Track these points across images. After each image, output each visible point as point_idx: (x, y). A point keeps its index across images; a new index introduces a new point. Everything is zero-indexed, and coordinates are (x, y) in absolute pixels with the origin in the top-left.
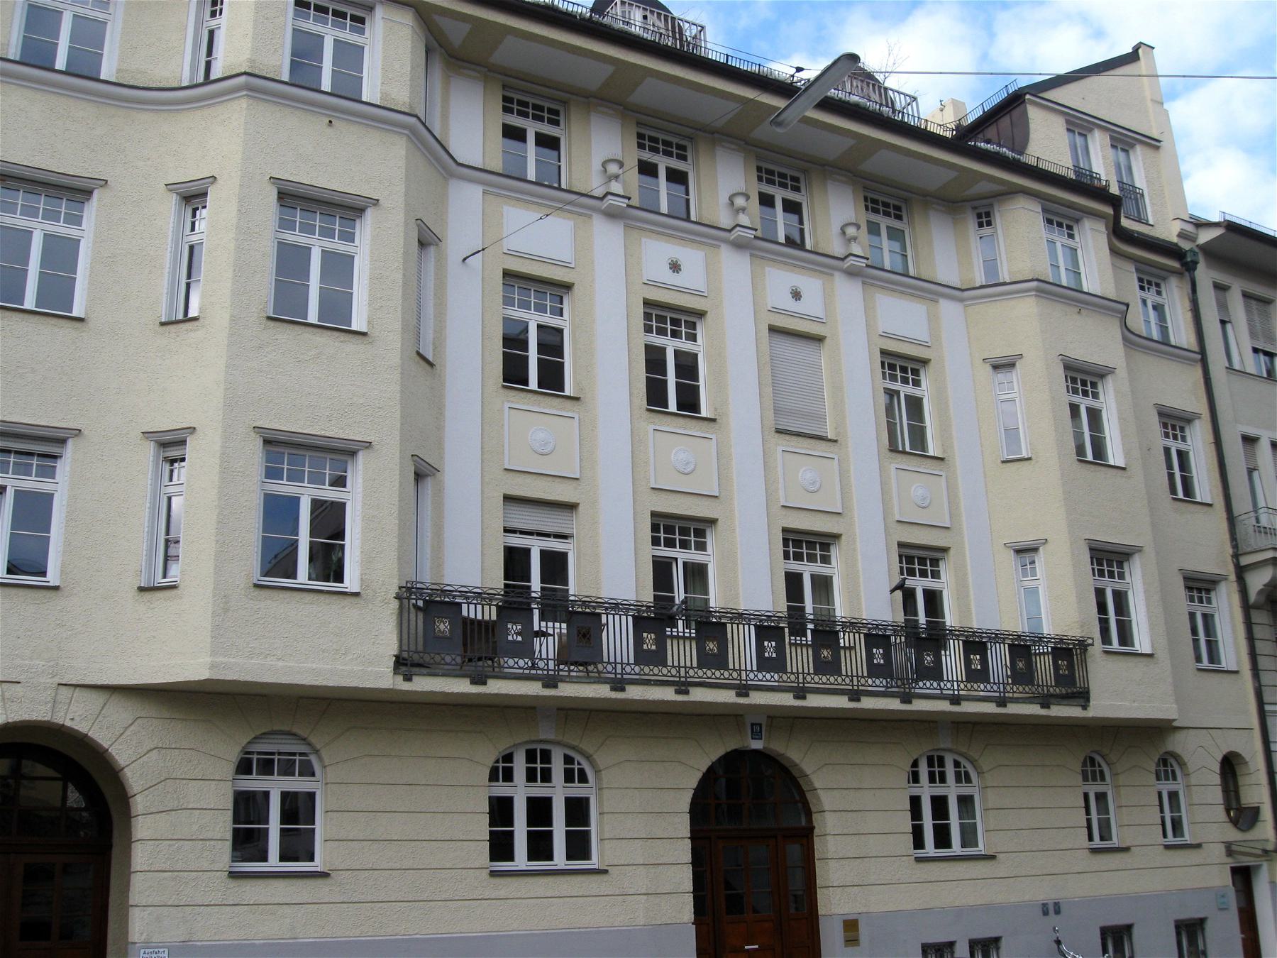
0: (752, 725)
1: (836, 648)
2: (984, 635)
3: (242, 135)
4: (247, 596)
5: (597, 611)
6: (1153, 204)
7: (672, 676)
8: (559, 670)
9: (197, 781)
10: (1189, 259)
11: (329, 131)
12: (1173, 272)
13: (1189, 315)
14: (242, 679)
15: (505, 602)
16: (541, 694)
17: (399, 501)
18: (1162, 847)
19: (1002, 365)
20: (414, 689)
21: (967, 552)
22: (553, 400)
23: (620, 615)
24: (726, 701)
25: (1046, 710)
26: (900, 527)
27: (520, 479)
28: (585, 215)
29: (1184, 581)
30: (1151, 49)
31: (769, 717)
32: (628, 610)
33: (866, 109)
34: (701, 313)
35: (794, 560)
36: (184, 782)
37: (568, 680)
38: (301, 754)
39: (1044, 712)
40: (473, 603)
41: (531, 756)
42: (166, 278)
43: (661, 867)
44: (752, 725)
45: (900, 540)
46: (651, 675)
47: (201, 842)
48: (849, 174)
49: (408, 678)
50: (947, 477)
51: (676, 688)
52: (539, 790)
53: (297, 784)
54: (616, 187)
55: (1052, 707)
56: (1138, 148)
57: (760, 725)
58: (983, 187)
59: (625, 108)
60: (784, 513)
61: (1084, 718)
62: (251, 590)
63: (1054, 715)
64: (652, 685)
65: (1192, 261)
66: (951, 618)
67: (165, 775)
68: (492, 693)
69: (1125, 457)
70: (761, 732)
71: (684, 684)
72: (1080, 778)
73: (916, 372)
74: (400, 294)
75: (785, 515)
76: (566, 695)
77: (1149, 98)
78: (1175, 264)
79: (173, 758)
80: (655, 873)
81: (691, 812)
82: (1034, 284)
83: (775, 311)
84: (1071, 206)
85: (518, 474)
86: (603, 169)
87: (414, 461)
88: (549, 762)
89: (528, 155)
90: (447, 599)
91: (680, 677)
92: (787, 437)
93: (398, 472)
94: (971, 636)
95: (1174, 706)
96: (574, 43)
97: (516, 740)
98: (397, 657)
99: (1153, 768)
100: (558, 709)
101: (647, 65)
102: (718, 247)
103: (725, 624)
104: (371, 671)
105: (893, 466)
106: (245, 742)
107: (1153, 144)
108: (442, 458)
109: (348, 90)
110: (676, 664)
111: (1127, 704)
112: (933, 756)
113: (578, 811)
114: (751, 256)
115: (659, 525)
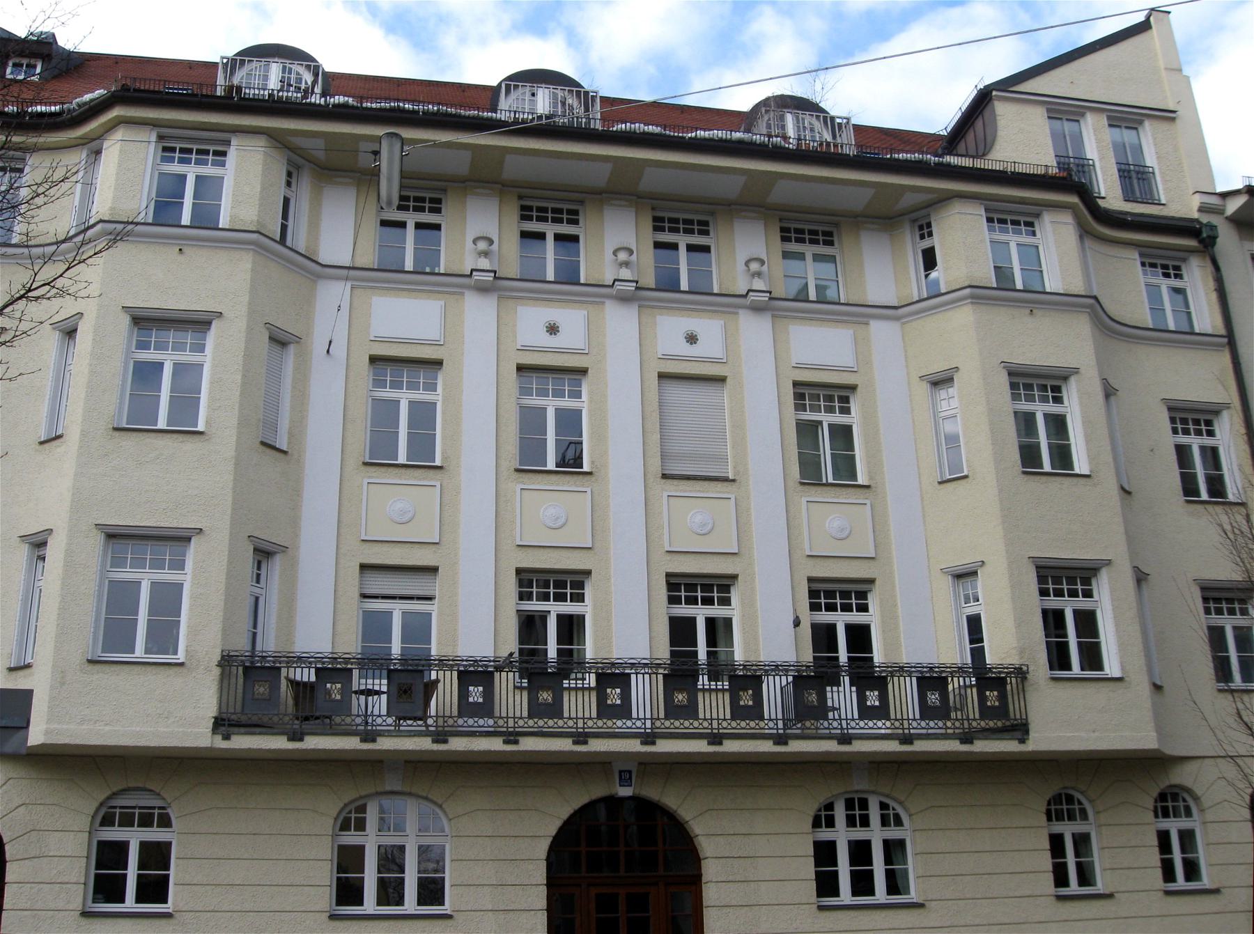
0: (620, 772)
1: (693, 692)
2: (913, 669)
3: (101, 274)
4: (81, 671)
5: (626, 671)
6: (1165, 181)
7: (638, 728)
8: (400, 725)
9: (58, 832)
10: (1204, 235)
11: (181, 258)
12: (1191, 251)
13: (1214, 296)
14: (72, 742)
15: (558, 669)
16: (359, 748)
17: (226, 579)
18: (1162, 892)
19: (941, 381)
20: (232, 747)
21: (897, 582)
22: (415, 472)
23: (780, 676)
24: (561, 749)
25: (969, 745)
26: (812, 561)
27: (377, 548)
28: (597, 303)
29: (1202, 591)
30: (1166, 14)
31: (640, 764)
32: (787, 671)
33: (752, 143)
34: (584, 370)
35: (685, 604)
36: (47, 833)
37: (386, 734)
38: (160, 808)
39: (436, 747)
40: (235, 666)
41: (849, 804)
42: (46, 406)
43: (512, 913)
44: (620, 772)
45: (810, 575)
46: (555, 728)
47: (59, 885)
48: (761, 209)
49: (227, 737)
50: (736, 499)
51: (504, 738)
52: (859, 834)
53: (155, 834)
54: (759, 284)
55: (975, 741)
56: (1147, 124)
57: (630, 772)
58: (908, 200)
59: (503, 186)
60: (668, 558)
61: (1021, 753)
62: (86, 665)
63: (978, 750)
64: (478, 736)
65: (1209, 237)
66: (590, 649)
67: (32, 828)
68: (309, 748)
69: (1090, 463)
70: (630, 778)
71: (510, 734)
72: (1044, 818)
73: (1209, 423)
74: (238, 393)
75: (670, 560)
76: (384, 748)
77: (1162, 67)
78: (1192, 243)
79: (38, 812)
80: (505, 918)
81: (548, 859)
82: (968, 291)
83: (666, 358)
84: (1022, 201)
85: (375, 544)
86: (747, 268)
87: (251, 541)
88: (867, 809)
89: (407, 246)
90: (617, 671)
91: (712, 729)
92: (675, 482)
93: (227, 553)
94: (470, 665)
95: (1155, 734)
96: (421, 138)
97: (832, 790)
98: (216, 718)
99: (1150, 803)
100: (406, 762)
101: (679, 160)
102: (737, 313)
103: (629, 675)
104: (191, 732)
105: (804, 500)
106: (102, 797)
107: (1167, 116)
108: (296, 535)
109: (206, 219)
110: (708, 716)
111: (1083, 734)
112: (853, 799)
113: (894, 850)
114: (772, 317)
115: (533, 580)
